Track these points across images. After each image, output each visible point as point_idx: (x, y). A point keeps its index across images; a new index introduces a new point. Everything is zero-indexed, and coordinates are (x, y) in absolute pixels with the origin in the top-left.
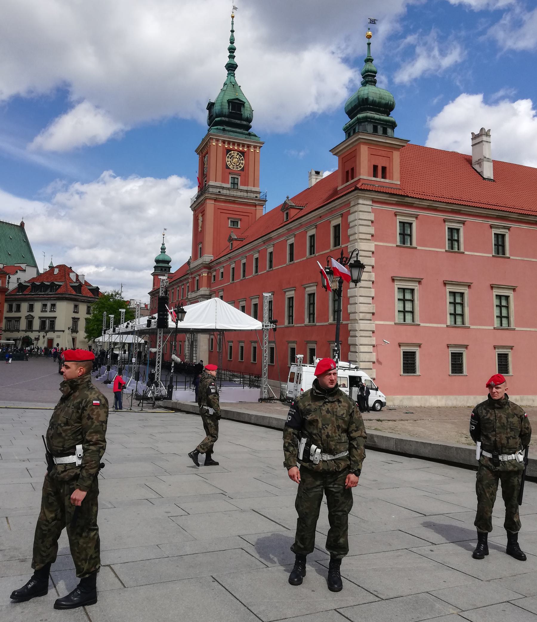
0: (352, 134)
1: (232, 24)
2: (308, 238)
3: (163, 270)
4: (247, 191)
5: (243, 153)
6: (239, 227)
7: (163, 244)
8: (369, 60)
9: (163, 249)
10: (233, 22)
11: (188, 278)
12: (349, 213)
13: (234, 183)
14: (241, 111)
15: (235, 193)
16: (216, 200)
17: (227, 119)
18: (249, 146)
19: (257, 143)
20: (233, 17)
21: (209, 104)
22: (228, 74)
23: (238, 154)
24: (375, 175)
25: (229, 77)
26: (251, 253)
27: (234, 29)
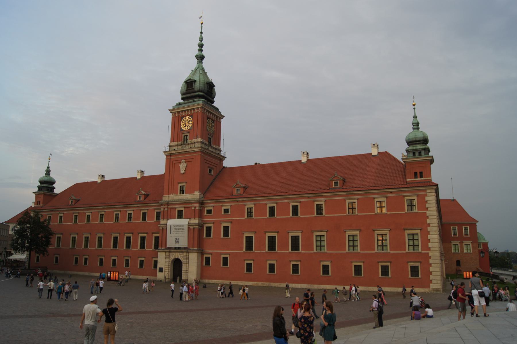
1: (202, 28)
2: (376, 202)
4: (216, 149)
5: (213, 121)
6: (212, 174)
7: (48, 167)
8: (415, 117)
9: (48, 172)
10: (202, 27)
12: (426, 195)
14: (212, 91)
15: (210, 149)
16: (204, 153)
17: (206, 95)
18: (217, 117)
20: (202, 23)
21: (189, 80)
22: (198, 63)
26: (286, 201)
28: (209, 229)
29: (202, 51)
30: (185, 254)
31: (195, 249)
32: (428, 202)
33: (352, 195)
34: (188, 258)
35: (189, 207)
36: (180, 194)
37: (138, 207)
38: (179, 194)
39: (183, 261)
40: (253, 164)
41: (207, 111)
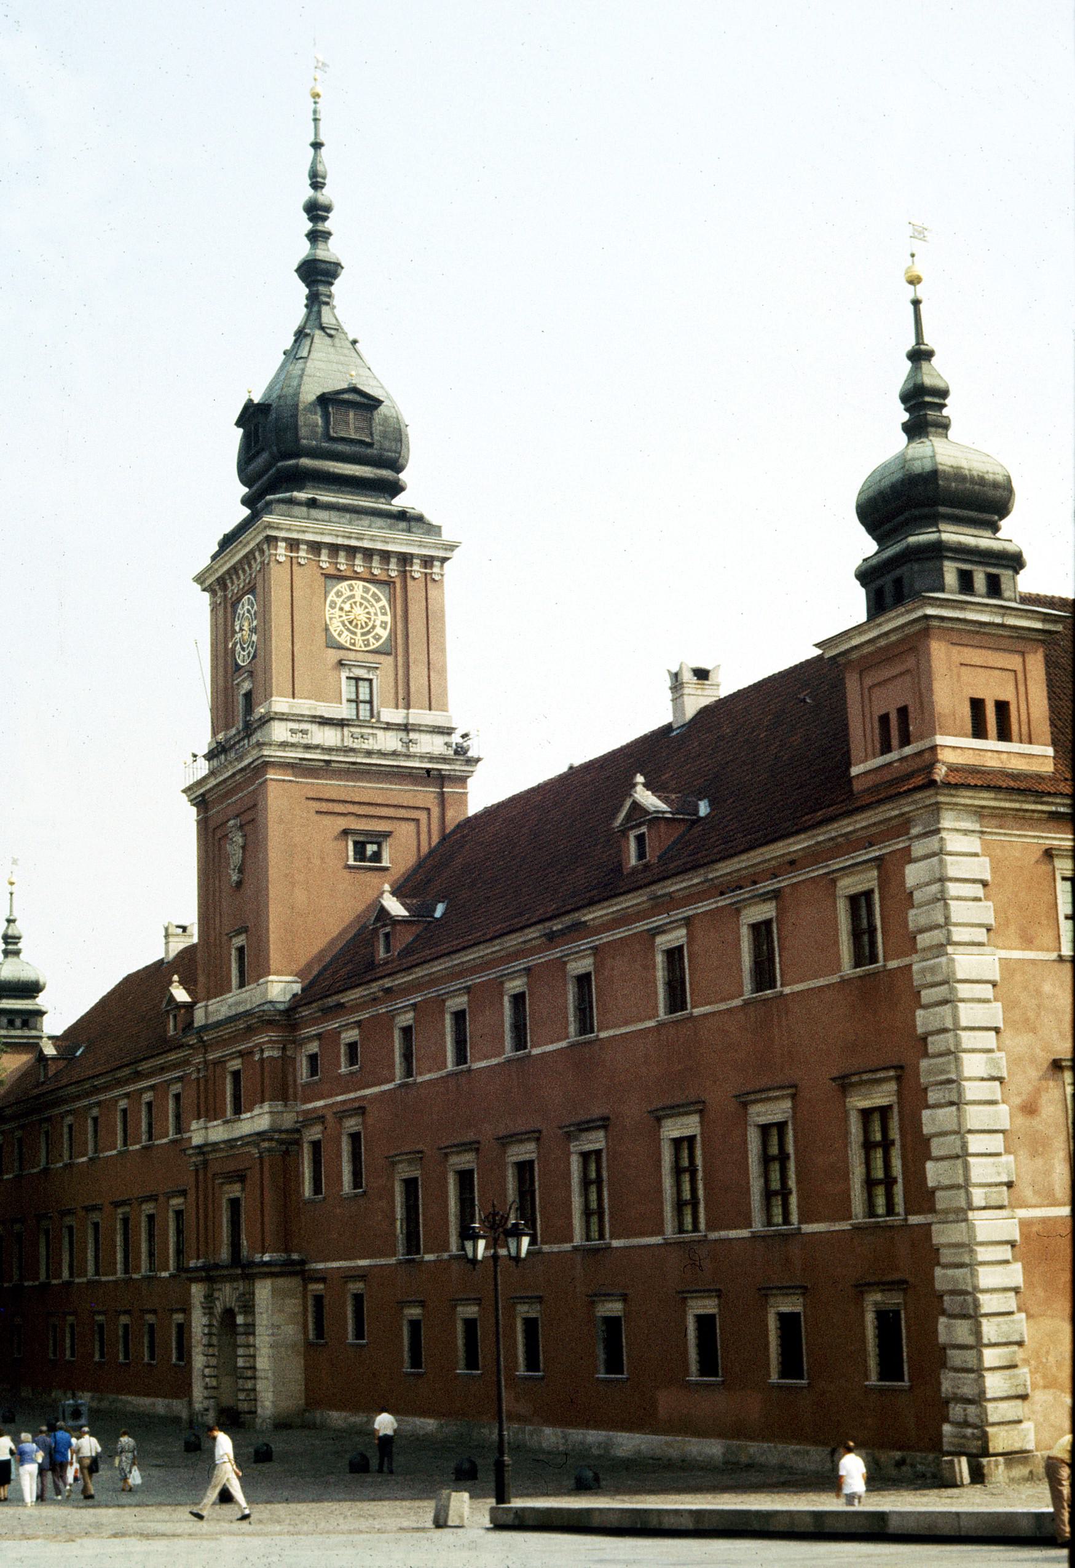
0: (889, 600)
3: (18, 1022)
4: (406, 728)
6: (385, 863)
10: (315, 112)
11: (186, 1062)
13: (357, 701)
18: (405, 559)
19: (436, 547)
23: (366, 590)
24: (979, 732)
25: (315, 309)
27: (322, 138)
28: (316, 1146)
29: (327, 235)
30: (241, 1286)
31: (266, 1258)
32: (918, 896)
33: (669, 903)
34: (249, 1308)
35: (251, 1053)
36: (242, 985)
37: (163, 1069)
38: (235, 991)
39: (240, 1320)
40: (564, 769)
41: (315, 547)
